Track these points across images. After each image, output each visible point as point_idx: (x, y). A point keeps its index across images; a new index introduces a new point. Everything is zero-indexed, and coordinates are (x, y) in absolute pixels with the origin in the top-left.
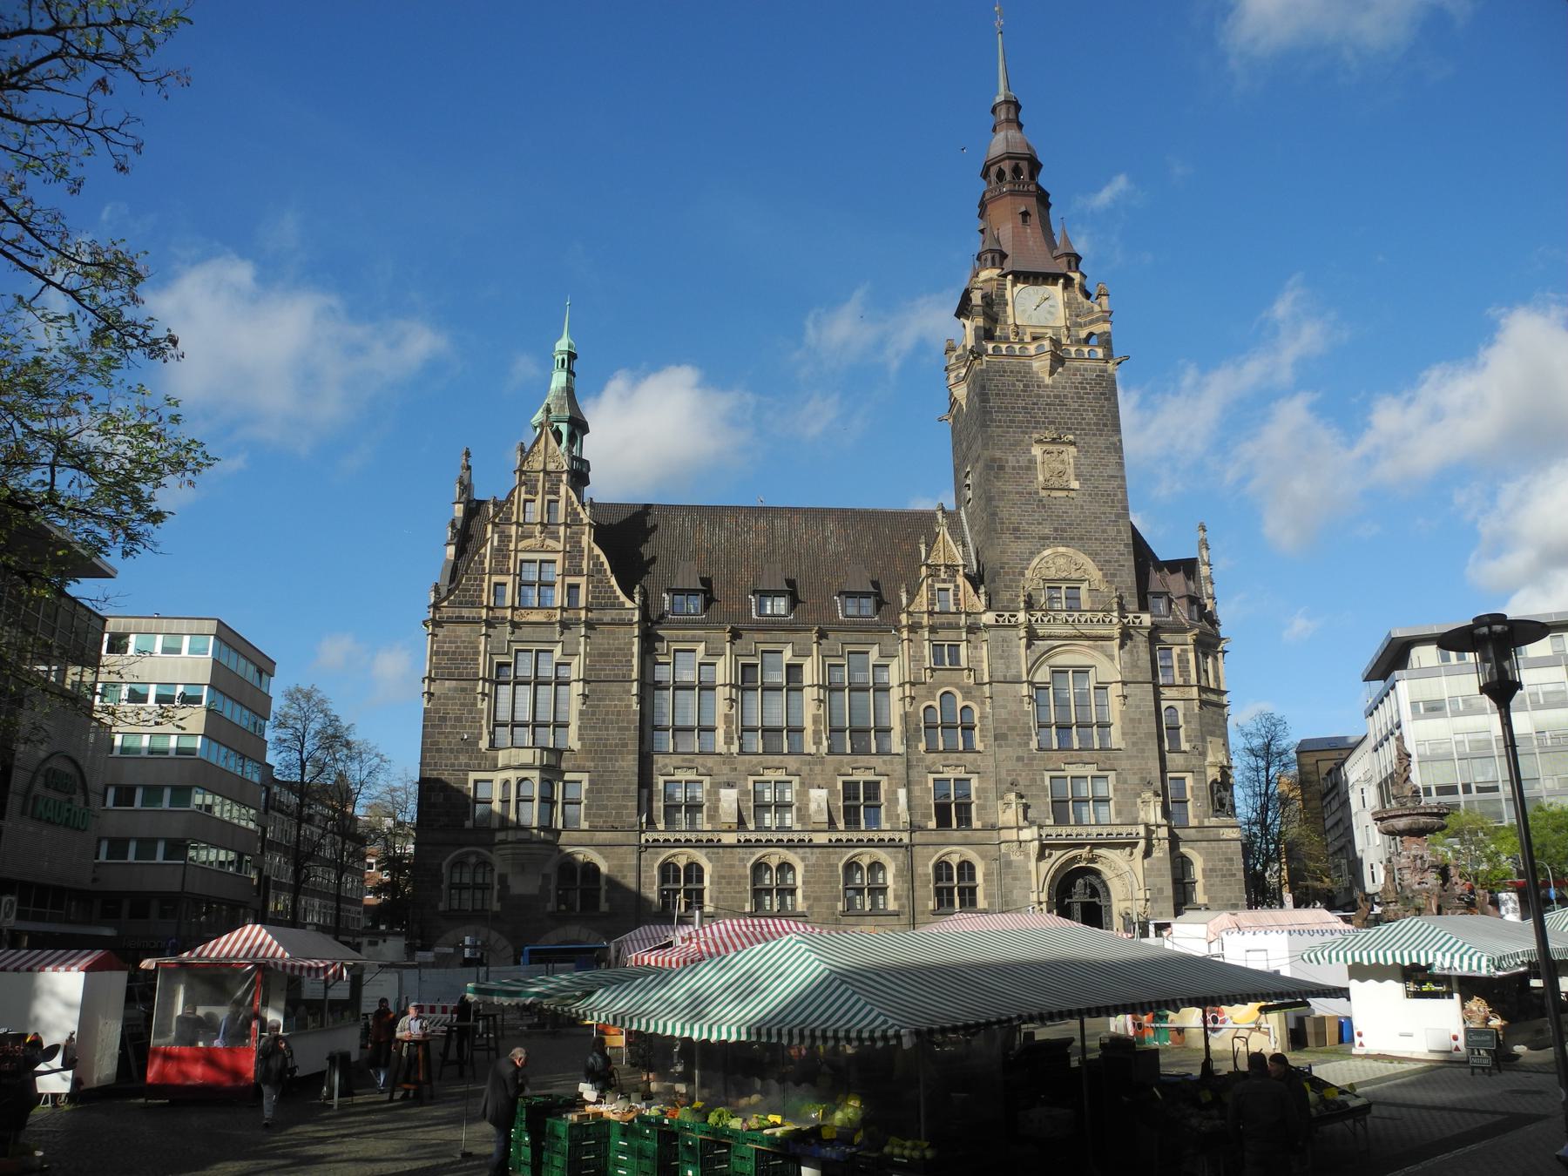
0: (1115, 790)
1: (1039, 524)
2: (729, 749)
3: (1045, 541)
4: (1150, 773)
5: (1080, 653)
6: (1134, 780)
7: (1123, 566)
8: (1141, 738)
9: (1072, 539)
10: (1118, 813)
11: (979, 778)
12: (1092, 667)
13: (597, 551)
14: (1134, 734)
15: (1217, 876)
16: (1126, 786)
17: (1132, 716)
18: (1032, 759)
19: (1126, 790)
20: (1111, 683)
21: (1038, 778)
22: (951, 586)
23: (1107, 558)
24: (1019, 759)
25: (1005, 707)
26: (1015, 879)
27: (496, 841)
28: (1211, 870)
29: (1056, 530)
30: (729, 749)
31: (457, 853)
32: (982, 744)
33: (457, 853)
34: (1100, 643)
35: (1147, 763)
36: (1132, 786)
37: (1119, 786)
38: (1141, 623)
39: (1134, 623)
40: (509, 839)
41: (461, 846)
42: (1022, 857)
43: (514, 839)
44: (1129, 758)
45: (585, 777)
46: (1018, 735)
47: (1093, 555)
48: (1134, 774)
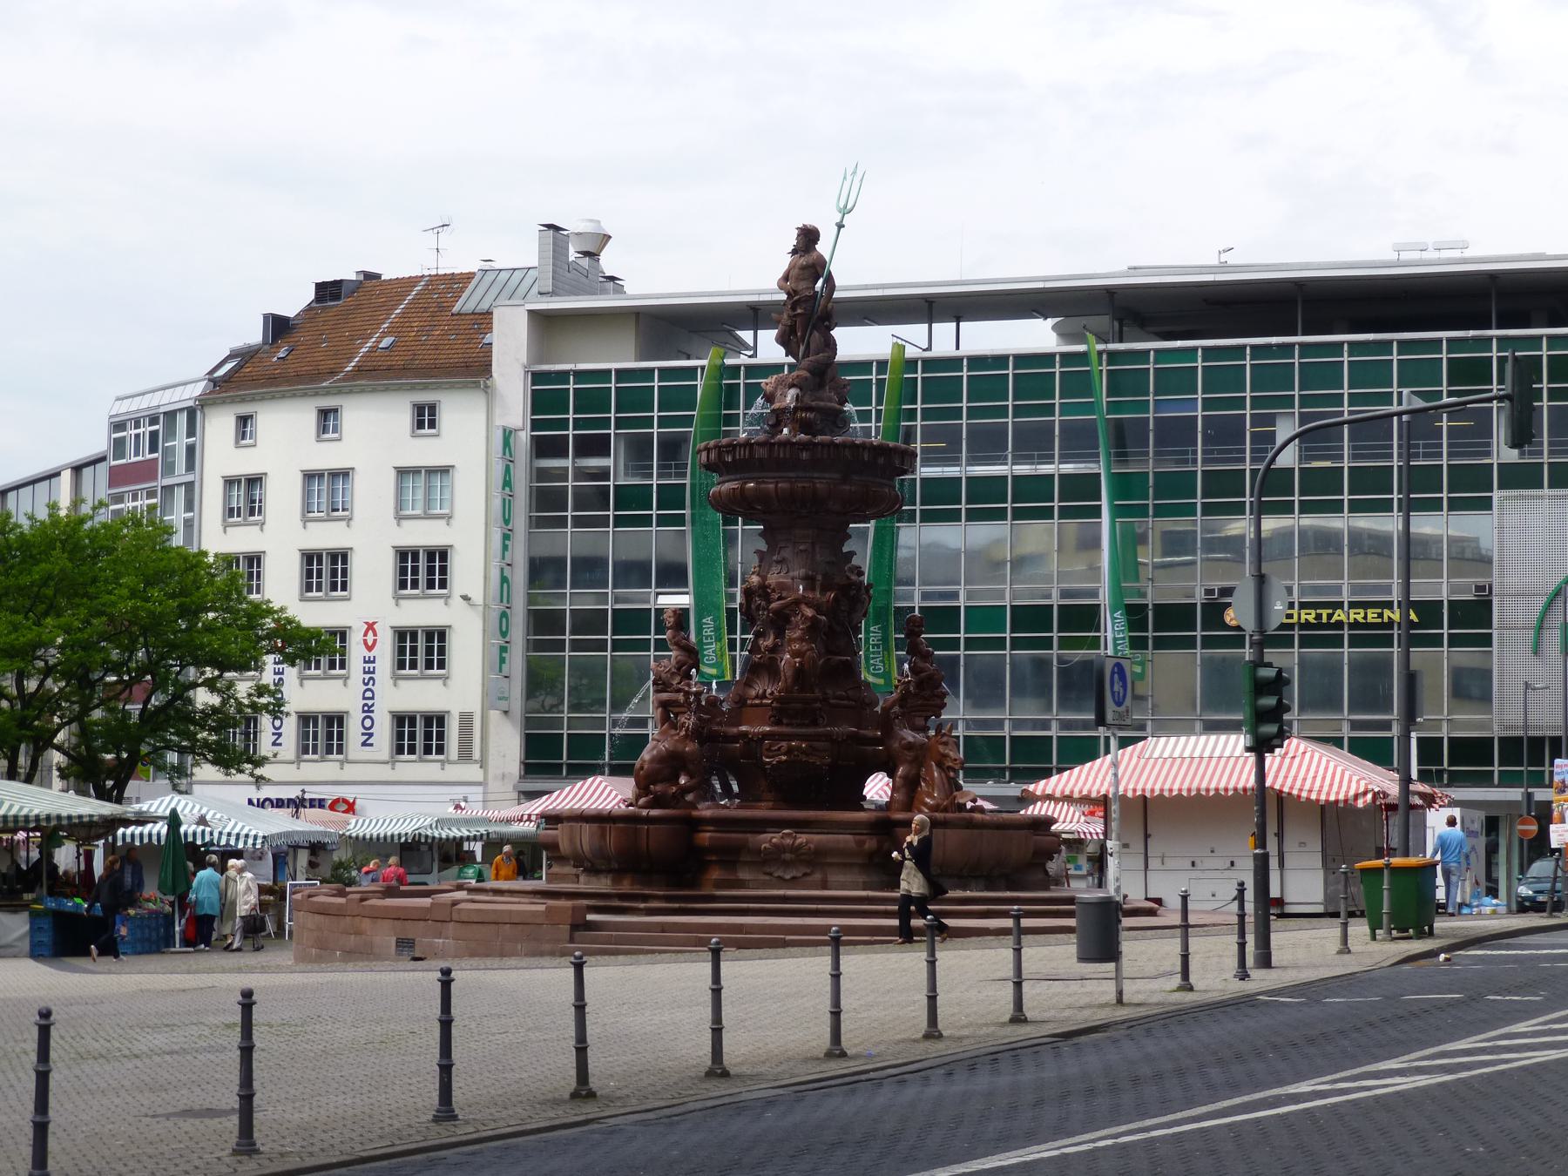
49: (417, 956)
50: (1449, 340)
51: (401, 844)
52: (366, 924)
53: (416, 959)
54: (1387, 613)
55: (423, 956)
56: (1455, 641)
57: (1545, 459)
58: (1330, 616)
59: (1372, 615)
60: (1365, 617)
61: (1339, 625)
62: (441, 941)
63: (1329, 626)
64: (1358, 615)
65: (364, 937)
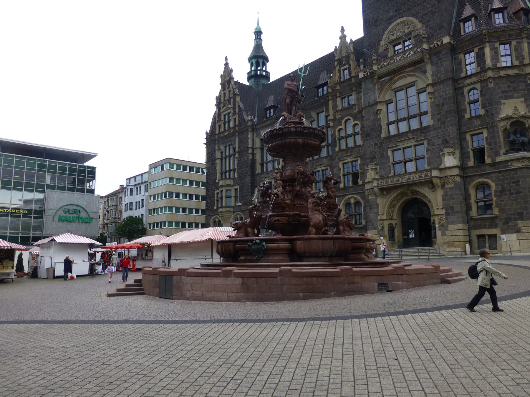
0: (427, 150)
1: (388, 12)
2: (279, 167)
3: (390, 20)
4: (449, 136)
5: (408, 76)
6: (438, 142)
7: (435, 12)
8: (443, 115)
9: (404, 12)
10: (429, 164)
11: (361, 159)
12: (415, 82)
13: (240, 103)
14: (439, 114)
15: (506, 195)
16: (434, 147)
17: (437, 103)
18: (382, 143)
19: (434, 149)
20: (426, 87)
21: (385, 153)
22: (347, 66)
23: (425, 12)
24: (376, 144)
25: (369, 119)
26: (371, 208)
27: (219, 212)
28: (501, 191)
29: (396, 11)
30: (279, 167)
31: (213, 217)
32: (362, 141)
33: (213, 217)
34: (418, 66)
35: (447, 130)
36: (438, 146)
37: (430, 147)
38: (442, 42)
39: (438, 45)
40: (223, 211)
41: (214, 215)
42: (374, 197)
43: (225, 211)
44: (435, 129)
45: (238, 187)
46: (375, 132)
47: (415, 16)
48: (439, 138)
49: (390, 289)
50: (38, 159)
51: (37, 254)
52: (358, 279)
53: (388, 291)
54: (20, 211)
55: (393, 289)
56: (34, 217)
57: (56, 185)
58: (7, 211)
59: (17, 211)
60: (15, 211)
61: (9, 212)
62: (400, 282)
63: (7, 212)
64: (13, 211)
65: (355, 285)
